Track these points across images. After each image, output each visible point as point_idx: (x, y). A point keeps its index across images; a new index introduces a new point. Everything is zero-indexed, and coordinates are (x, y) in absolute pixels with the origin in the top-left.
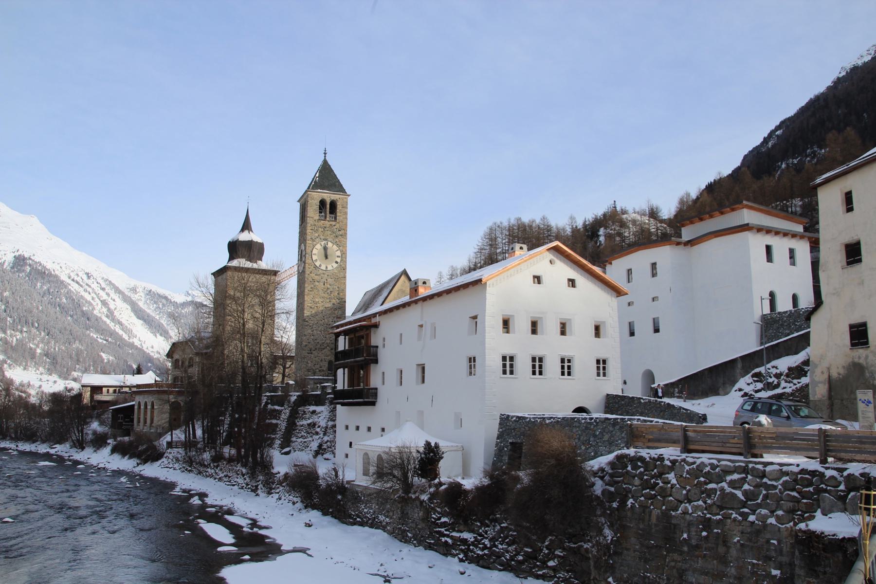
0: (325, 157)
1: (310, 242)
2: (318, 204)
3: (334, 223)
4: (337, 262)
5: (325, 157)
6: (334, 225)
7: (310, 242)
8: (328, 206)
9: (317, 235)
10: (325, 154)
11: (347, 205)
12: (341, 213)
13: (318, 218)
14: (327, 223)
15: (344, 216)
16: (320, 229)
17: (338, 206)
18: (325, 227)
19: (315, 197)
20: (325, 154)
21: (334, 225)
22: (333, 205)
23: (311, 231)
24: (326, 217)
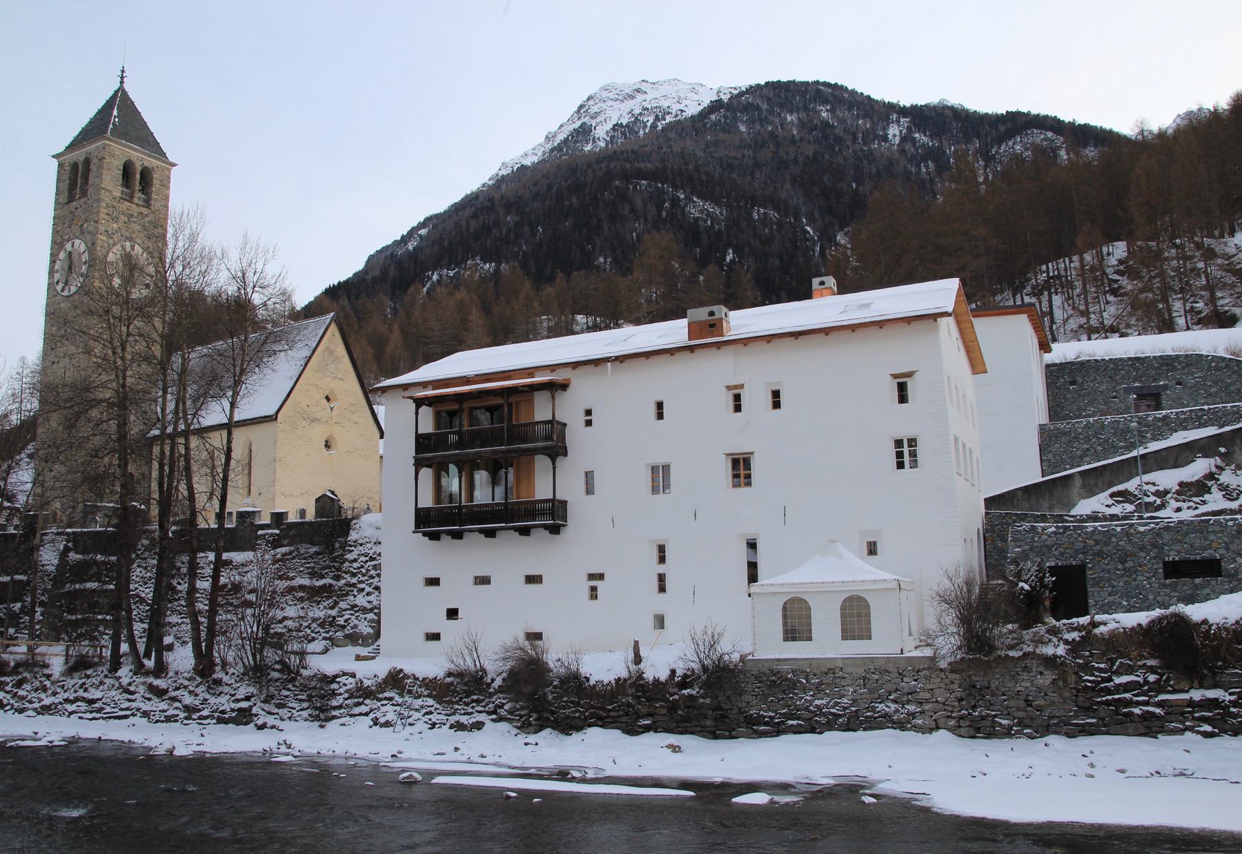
0: (122, 82)
1: (105, 238)
2: (122, 168)
3: (145, 211)
4: (147, 286)
5: (122, 82)
6: (146, 216)
7: (105, 238)
8: (138, 176)
9: (115, 226)
10: (122, 78)
11: (169, 182)
12: (158, 195)
13: (120, 195)
14: (135, 210)
15: (163, 203)
16: (122, 217)
17: (155, 181)
18: (132, 216)
19: (117, 153)
20: (122, 78)
21: (146, 216)
22: (146, 175)
23: (106, 217)
24: (132, 196)
